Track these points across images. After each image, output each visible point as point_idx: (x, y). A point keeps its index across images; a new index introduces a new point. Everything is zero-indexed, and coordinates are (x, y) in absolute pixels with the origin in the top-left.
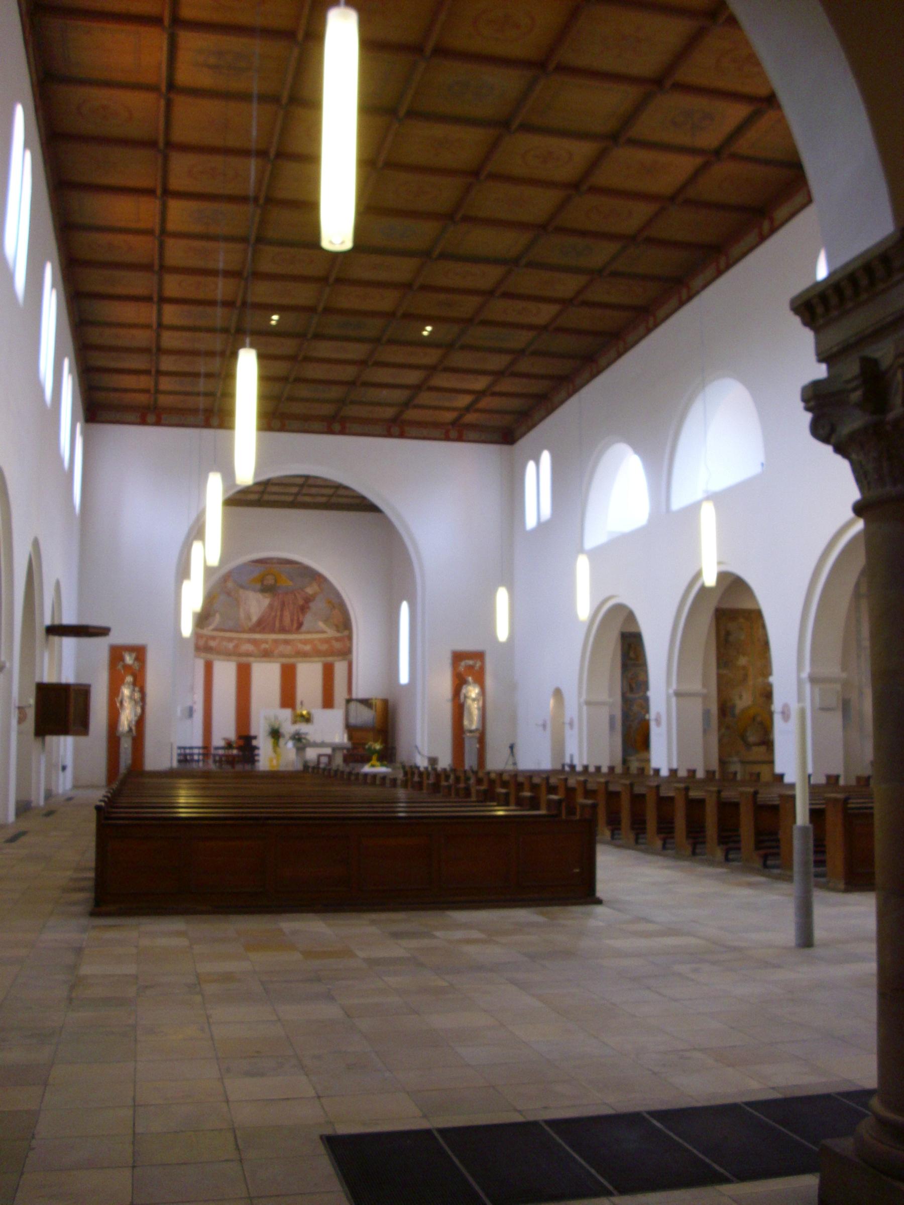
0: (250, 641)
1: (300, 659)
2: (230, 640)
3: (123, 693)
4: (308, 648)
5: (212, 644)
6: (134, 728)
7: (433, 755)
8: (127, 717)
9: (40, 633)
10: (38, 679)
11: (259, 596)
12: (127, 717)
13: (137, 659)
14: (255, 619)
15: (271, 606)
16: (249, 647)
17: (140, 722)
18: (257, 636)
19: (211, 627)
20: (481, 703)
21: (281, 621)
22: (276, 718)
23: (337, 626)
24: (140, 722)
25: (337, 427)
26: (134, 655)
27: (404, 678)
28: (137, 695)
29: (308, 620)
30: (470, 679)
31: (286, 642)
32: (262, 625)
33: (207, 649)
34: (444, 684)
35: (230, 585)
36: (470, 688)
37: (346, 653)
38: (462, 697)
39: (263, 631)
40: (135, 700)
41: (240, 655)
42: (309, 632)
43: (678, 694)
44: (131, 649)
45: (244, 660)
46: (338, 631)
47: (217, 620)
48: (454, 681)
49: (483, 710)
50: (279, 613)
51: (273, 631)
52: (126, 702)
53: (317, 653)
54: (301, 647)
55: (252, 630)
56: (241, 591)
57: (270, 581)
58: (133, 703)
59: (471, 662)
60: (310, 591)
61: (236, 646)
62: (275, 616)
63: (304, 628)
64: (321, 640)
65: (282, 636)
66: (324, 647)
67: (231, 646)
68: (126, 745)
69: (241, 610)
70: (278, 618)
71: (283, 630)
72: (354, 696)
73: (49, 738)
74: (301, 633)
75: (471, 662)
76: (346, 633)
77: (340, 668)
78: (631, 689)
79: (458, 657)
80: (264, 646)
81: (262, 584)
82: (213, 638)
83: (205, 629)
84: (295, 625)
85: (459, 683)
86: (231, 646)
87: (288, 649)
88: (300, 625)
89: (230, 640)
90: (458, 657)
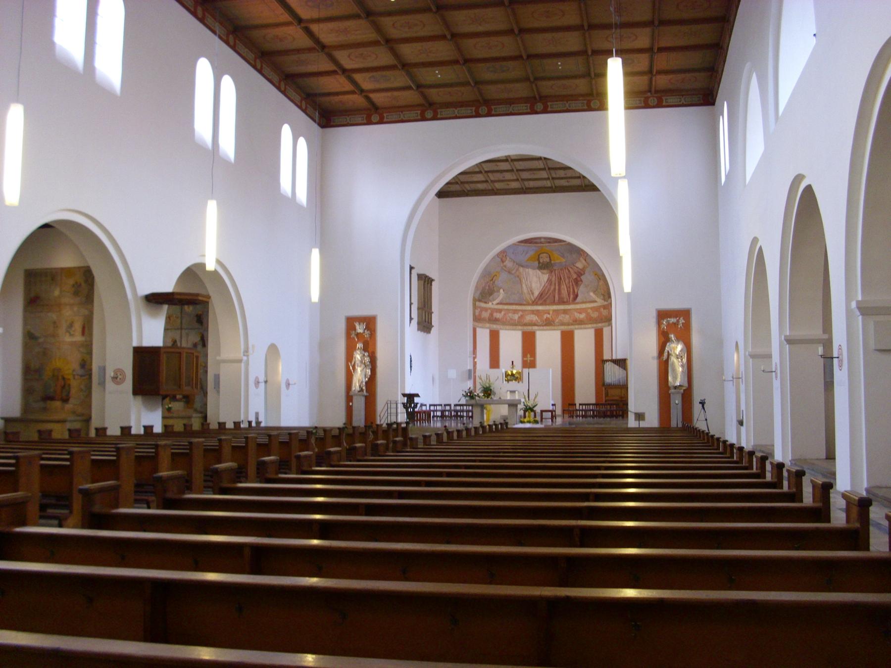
0: (533, 312)
1: (577, 326)
2: (515, 311)
4: (582, 316)
5: (497, 315)
6: (364, 388)
7: (640, 411)
10: (135, 344)
11: (538, 272)
13: (368, 328)
14: (536, 293)
15: (549, 281)
16: (534, 318)
17: (371, 383)
18: (540, 308)
20: (685, 360)
22: (488, 377)
23: (604, 295)
24: (371, 383)
25: (539, 106)
28: (367, 359)
29: (582, 290)
30: (672, 336)
31: (565, 312)
32: (542, 298)
33: (492, 320)
34: (649, 342)
35: (508, 264)
36: (673, 345)
37: (608, 320)
38: (666, 354)
39: (544, 303)
40: (365, 364)
41: (525, 325)
42: (583, 302)
44: (361, 320)
45: (529, 329)
47: (501, 295)
48: (659, 339)
50: (557, 287)
51: (554, 303)
53: (590, 320)
54: (577, 315)
55: (534, 303)
56: (521, 269)
57: (545, 259)
58: (363, 366)
59: (673, 320)
60: (580, 265)
61: (522, 317)
62: (555, 289)
63: (579, 299)
64: (591, 308)
66: (595, 315)
69: (524, 286)
70: (557, 291)
71: (562, 302)
72: (606, 356)
74: (578, 303)
77: (606, 331)
79: (662, 315)
80: (545, 316)
81: (539, 263)
82: (500, 311)
83: (490, 303)
84: (572, 296)
85: (664, 340)
86: (516, 317)
87: (566, 318)
88: (577, 296)
89: (515, 311)
90: (662, 315)
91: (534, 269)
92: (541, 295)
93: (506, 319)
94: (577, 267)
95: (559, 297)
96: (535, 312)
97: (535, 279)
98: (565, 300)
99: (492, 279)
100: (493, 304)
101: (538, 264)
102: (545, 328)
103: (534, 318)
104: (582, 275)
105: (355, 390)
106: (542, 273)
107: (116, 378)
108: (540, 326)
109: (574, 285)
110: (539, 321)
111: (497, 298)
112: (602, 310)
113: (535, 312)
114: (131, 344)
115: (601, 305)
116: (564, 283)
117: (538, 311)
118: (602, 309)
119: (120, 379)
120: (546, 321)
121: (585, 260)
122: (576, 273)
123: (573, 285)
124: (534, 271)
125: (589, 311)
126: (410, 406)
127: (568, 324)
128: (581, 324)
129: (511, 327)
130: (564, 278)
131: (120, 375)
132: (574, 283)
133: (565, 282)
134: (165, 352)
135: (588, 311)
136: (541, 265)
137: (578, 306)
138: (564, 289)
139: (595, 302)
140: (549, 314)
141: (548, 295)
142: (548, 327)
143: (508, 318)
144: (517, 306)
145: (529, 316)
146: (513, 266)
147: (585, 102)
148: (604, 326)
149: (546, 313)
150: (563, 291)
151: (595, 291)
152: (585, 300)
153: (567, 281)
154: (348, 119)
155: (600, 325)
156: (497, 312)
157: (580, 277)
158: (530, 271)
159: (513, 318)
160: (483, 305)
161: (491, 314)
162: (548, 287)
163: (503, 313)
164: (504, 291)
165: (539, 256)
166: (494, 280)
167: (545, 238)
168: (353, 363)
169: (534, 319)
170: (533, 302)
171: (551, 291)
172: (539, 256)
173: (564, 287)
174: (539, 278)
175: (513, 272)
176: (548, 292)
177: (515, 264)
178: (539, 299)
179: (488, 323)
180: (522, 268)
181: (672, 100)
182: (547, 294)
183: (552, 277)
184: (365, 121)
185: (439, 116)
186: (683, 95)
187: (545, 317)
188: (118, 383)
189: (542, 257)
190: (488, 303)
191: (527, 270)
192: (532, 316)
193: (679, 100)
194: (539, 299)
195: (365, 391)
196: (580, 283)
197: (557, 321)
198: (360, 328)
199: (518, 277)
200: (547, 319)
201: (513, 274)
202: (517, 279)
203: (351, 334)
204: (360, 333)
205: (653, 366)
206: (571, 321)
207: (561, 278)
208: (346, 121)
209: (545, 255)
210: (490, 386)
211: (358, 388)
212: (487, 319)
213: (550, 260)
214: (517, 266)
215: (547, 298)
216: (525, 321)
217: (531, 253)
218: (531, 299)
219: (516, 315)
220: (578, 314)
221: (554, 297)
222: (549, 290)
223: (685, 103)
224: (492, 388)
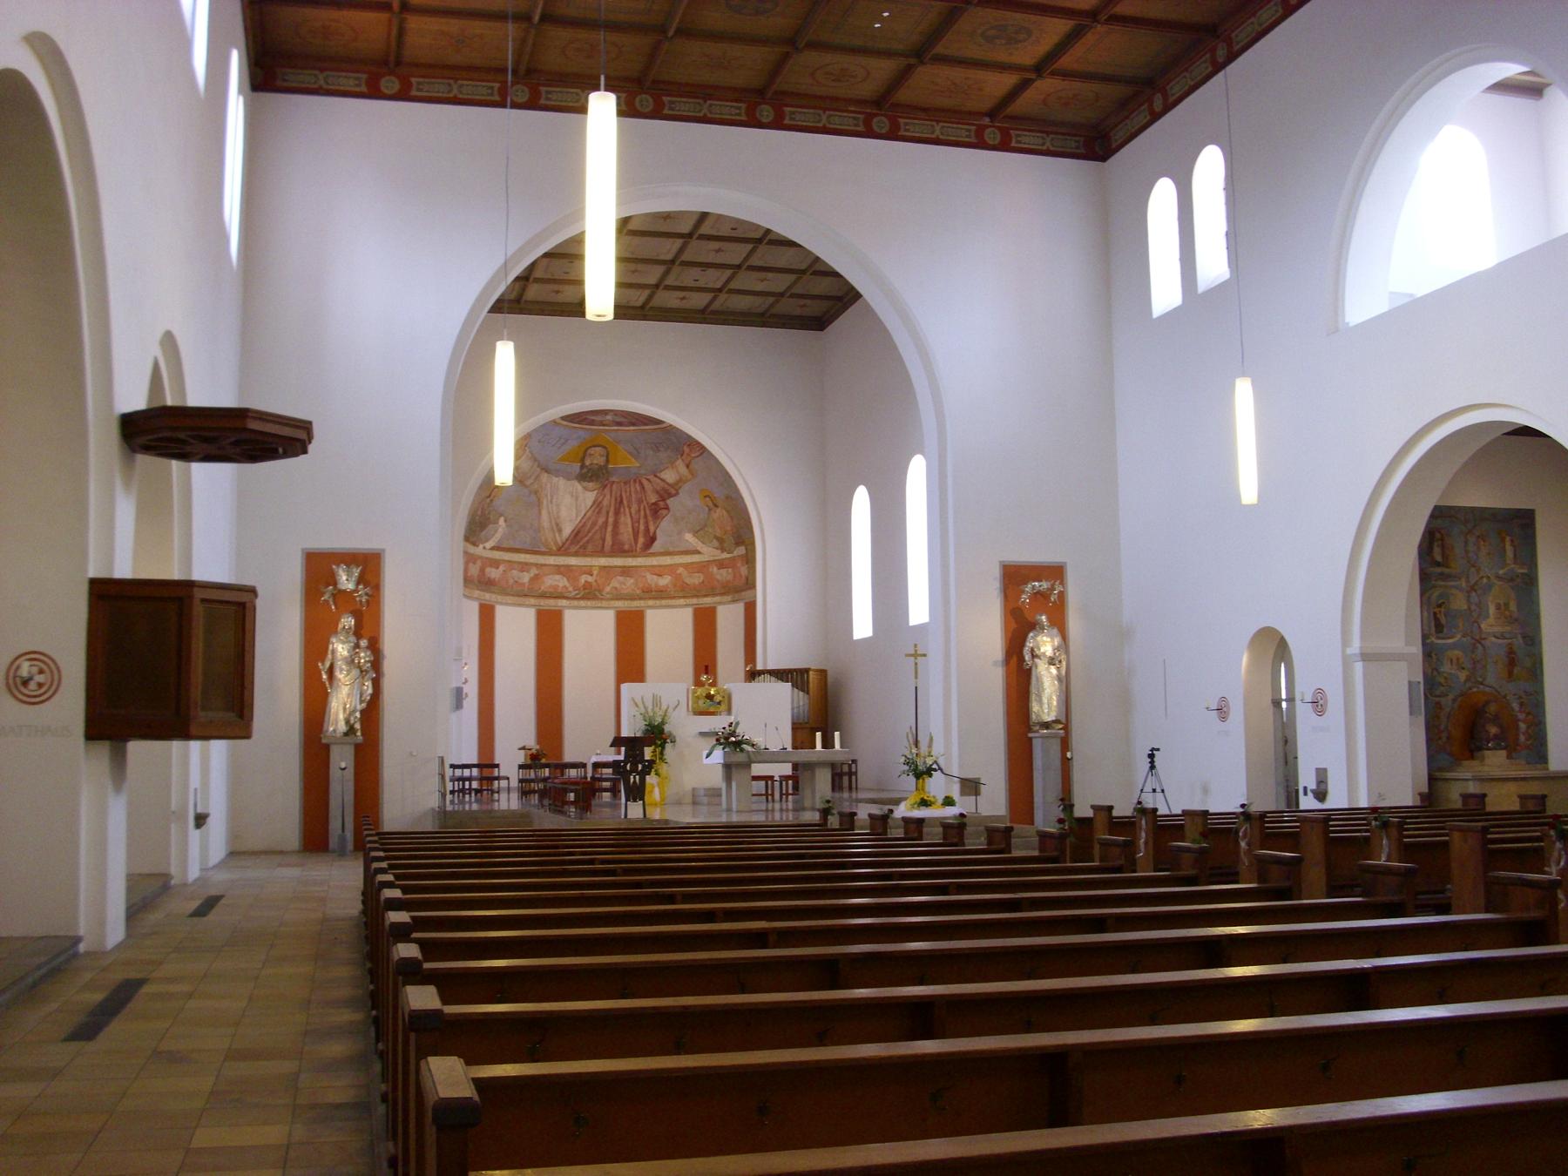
0: (560, 570)
1: (651, 602)
2: (524, 567)
3: (333, 652)
4: (665, 581)
5: (493, 573)
6: (358, 726)
7: (970, 774)
8: (343, 703)
9: (103, 441)
10: (93, 573)
11: (578, 486)
12: (343, 703)
14: (567, 530)
15: (597, 504)
16: (561, 582)
17: (371, 712)
18: (573, 561)
19: (489, 545)
21: (615, 533)
22: (656, 701)
23: (721, 540)
24: (371, 712)
25: (766, 113)
26: (356, 572)
27: (863, 626)
28: (364, 657)
29: (665, 530)
31: (626, 571)
32: (579, 542)
33: (486, 584)
37: (743, 587)
38: (1027, 657)
40: (359, 667)
41: (543, 596)
43: (1366, 657)
44: (350, 558)
46: (723, 550)
47: (500, 529)
49: (1065, 682)
50: (611, 520)
51: (601, 552)
52: (341, 670)
53: (683, 591)
54: (652, 579)
55: (562, 550)
56: (545, 477)
57: (596, 457)
58: (355, 672)
59: (1045, 585)
60: (669, 476)
61: (536, 578)
62: (606, 523)
63: (657, 546)
64: (686, 566)
65: (618, 561)
66: (696, 579)
67: (526, 578)
68: (342, 761)
69: (544, 512)
70: (610, 529)
71: (619, 550)
73: (138, 749)
74: (654, 554)
75: (1045, 585)
76: (741, 550)
78: (1439, 627)
79: (1014, 577)
80: (584, 579)
81: (582, 467)
82: (495, 563)
83: (481, 546)
84: (641, 540)
86: (526, 578)
88: (653, 539)
89: (524, 567)
90: (1014, 577)
91: (569, 480)
92: (576, 534)
93: (507, 582)
94: (663, 480)
95: (613, 542)
96: (562, 569)
97: (567, 500)
98: (626, 547)
99: (490, 496)
100: (484, 548)
101: (578, 470)
102: (582, 603)
103: (561, 582)
104: (671, 496)
105: (334, 731)
106: (585, 488)
107: (25, 683)
108: (574, 598)
109: (650, 518)
110: (571, 589)
111: (494, 535)
112: (714, 569)
113: (562, 569)
114: (86, 571)
115: (712, 559)
116: (627, 510)
117: (568, 567)
118: (715, 569)
119: (40, 685)
120: (584, 589)
121: (688, 466)
122: (657, 492)
123: (646, 517)
124: (569, 482)
125: (681, 570)
126: (634, 769)
127: (632, 598)
128: (662, 598)
129: (515, 599)
130: (629, 502)
131: (41, 672)
132: (648, 512)
133: (630, 508)
134: (204, 600)
135: (678, 572)
136: (585, 470)
137: (654, 561)
138: (626, 524)
139: (699, 553)
140: (592, 575)
141: (590, 534)
142: (589, 603)
143: (511, 581)
144: (528, 556)
145: (551, 576)
146: (532, 467)
147: (861, 116)
148: (720, 603)
149: (585, 573)
150: (622, 529)
151: (697, 532)
152: (671, 549)
153: (634, 507)
154: (321, 76)
155: (708, 601)
156: (491, 566)
157: (664, 500)
158: (561, 482)
159: (520, 581)
160: (472, 549)
161: (482, 570)
162: (593, 518)
163: (502, 568)
164: (505, 521)
165: (586, 451)
166: (492, 497)
167: (616, 413)
168: (328, 664)
169: (561, 585)
170: (559, 549)
171: (597, 528)
172: (586, 451)
173: (626, 522)
174: (577, 499)
175: (528, 483)
176: (591, 528)
177: (536, 463)
178: (571, 544)
179: (478, 589)
180: (546, 475)
181: (1030, 139)
182: (589, 532)
183: (603, 499)
184: (364, 89)
185: (543, 102)
186: (1048, 133)
187: (583, 581)
188: (33, 701)
189: (590, 455)
190: (478, 546)
191: (555, 480)
192: (557, 577)
193: (1041, 141)
194: (571, 544)
195: (359, 734)
196: (664, 512)
197: (608, 589)
198: (346, 580)
199: (536, 493)
200: (587, 585)
201: (526, 486)
202: (533, 497)
203: (323, 594)
204: (345, 591)
205: (994, 680)
206: (638, 592)
207: (621, 501)
208: (315, 83)
209: (597, 449)
210: (663, 723)
211: (342, 727)
212: (476, 581)
213: (607, 461)
214: (539, 469)
215: (588, 542)
216: (542, 588)
217: (573, 444)
218: (556, 543)
219: (525, 573)
220: (655, 577)
221: (604, 540)
222: (594, 524)
223: (1052, 148)
224: (667, 728)
